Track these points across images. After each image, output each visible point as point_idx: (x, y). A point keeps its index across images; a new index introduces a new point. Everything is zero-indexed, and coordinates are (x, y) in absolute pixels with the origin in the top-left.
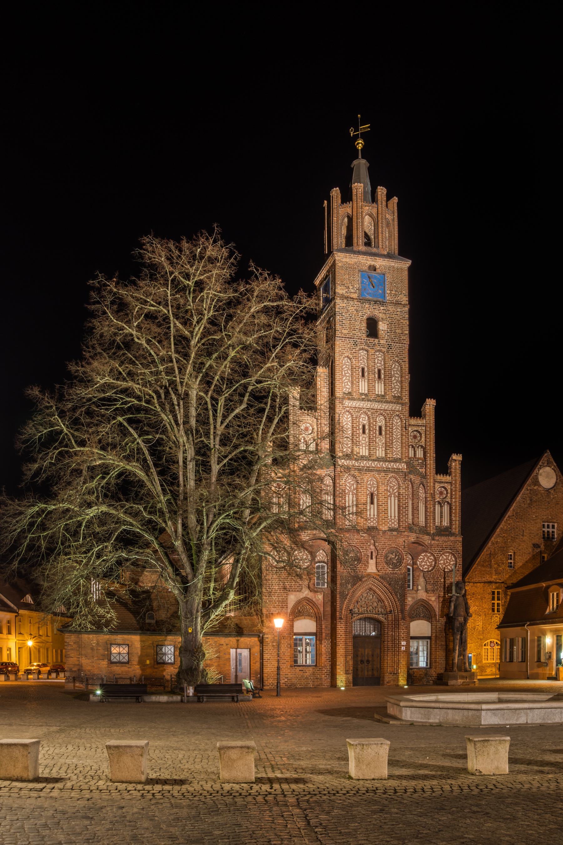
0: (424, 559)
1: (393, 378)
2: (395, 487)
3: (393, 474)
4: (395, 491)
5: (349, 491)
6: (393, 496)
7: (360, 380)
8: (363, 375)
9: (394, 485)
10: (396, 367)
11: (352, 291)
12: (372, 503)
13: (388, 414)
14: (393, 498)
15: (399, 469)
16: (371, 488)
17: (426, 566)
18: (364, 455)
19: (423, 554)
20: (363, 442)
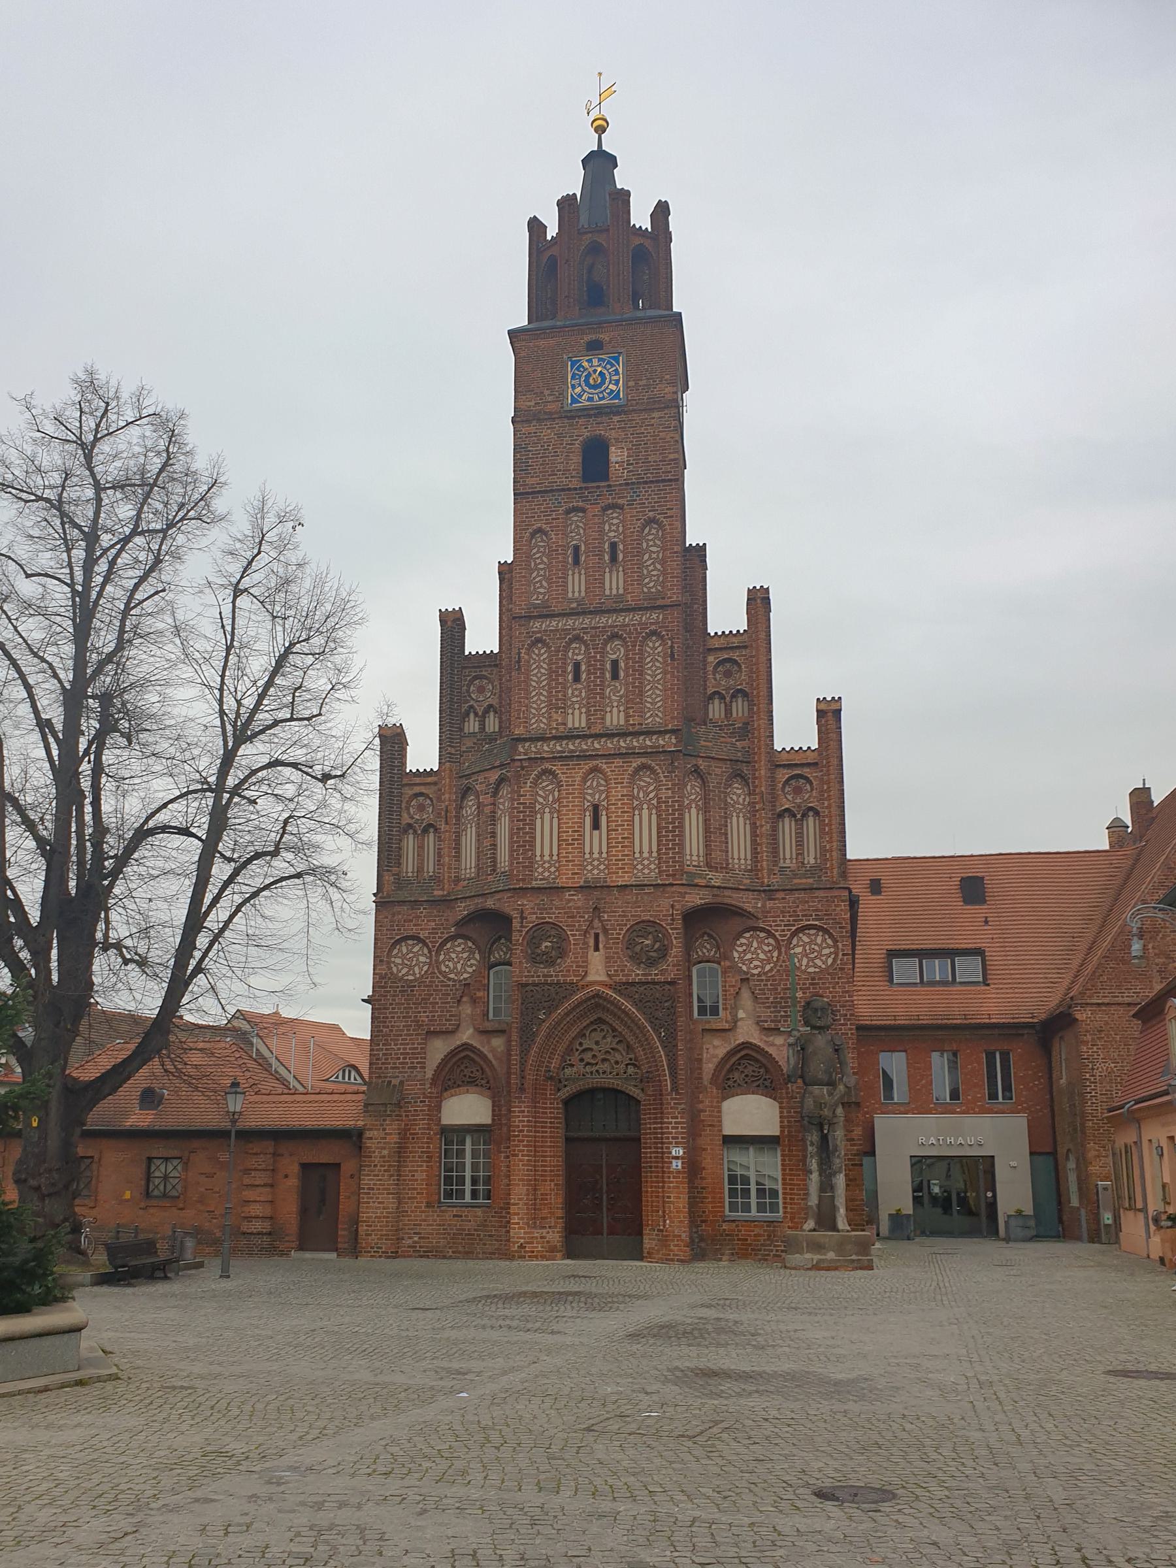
0: (750, 945)
1: (646, 557)
2: (652, 788)
3: (644, 760)
4: (651, 795)
5: (544, 806)
6: (645, 806)
7: (570, 572)
8: (576, 562)
9: (649, 783)
10: (654, 531)
11: (550, 398)
12: (596, 826)
13: (630, 633)
14: (645, 812)
15: (658, 747)
16: (592, 795)
17: (756, 963)
18: (577, 725)
19: (747, 935)
20: (574, 699)
